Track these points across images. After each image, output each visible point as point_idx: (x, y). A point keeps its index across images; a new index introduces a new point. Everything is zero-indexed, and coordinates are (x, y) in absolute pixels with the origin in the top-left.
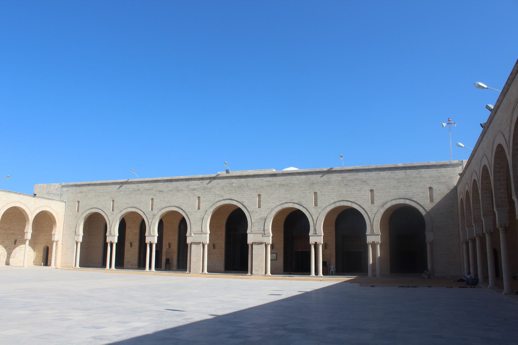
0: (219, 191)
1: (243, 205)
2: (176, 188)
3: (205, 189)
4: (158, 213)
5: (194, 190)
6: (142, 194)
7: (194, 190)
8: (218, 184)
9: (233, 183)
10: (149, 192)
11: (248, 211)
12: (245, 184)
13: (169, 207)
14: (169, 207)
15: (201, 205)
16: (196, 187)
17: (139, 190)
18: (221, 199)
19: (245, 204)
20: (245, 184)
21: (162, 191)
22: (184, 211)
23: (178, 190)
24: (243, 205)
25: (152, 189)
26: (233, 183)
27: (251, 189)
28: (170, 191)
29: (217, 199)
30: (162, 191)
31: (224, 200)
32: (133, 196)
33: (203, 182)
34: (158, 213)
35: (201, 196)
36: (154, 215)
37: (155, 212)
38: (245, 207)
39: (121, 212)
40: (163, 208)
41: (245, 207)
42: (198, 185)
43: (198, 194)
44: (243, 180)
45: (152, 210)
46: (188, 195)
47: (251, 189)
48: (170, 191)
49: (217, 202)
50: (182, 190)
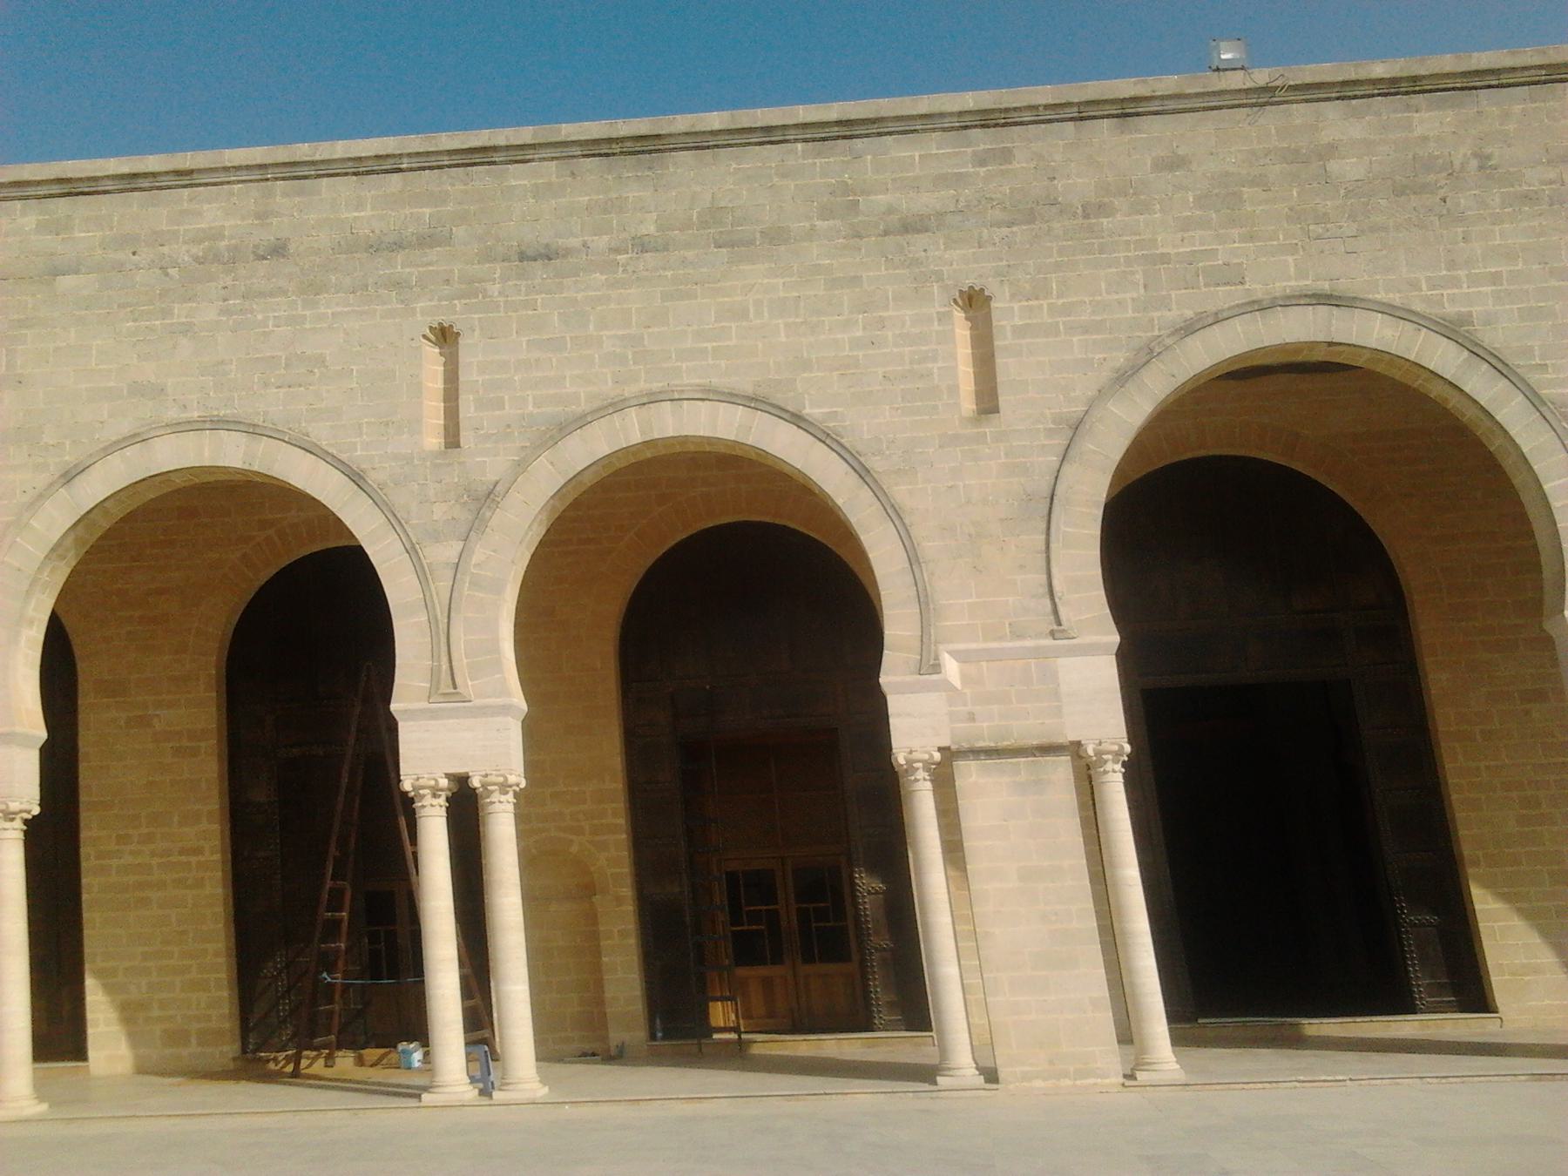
0: (1186, 225)
1: (1478, 352)
2: (714, 214)
3: (1030, 217)
4: (521, 466)
5: (912, 226)
6: (312, 289)
7: (912, 226)
8: (1175, 163)
9: (1332, 150)
10: (400, 266)
11: (1535, 399)
12: (1461, 153)
13: (652, 399)
14: (652, 399)
15: (1007, 367)
16: (927, 201)
17: (278, 250)
18: (1224, 297)
19: (1491, 338)
20: (1461, 153)
21: (548, 255)
22: (825, 437)
23: (734, 238)
24: (1478, 352)
25: (427, 241)
26: (1332, 150)
27: (1527, 198)
28: (642, 246)
29: (1177, 313)
30: (548, 255)
31: (1261, 307)
32: (209, 313)
33: (1006, 155)
34: (521, 466)
35: (992, 287)
36: (486, 499)
37: (486, 461)
38: (1502, 368)
39: (69, 477)
40: (582, 421)
41: (1502, 368)
42: (941, 181)
43: (963, 264)
44: (1430, 121)
45: (452, 439)
46: (855, 281)
47: (1527, 198)
48: (642, 246)
49: (1188, 329)
50: (776, 236)
